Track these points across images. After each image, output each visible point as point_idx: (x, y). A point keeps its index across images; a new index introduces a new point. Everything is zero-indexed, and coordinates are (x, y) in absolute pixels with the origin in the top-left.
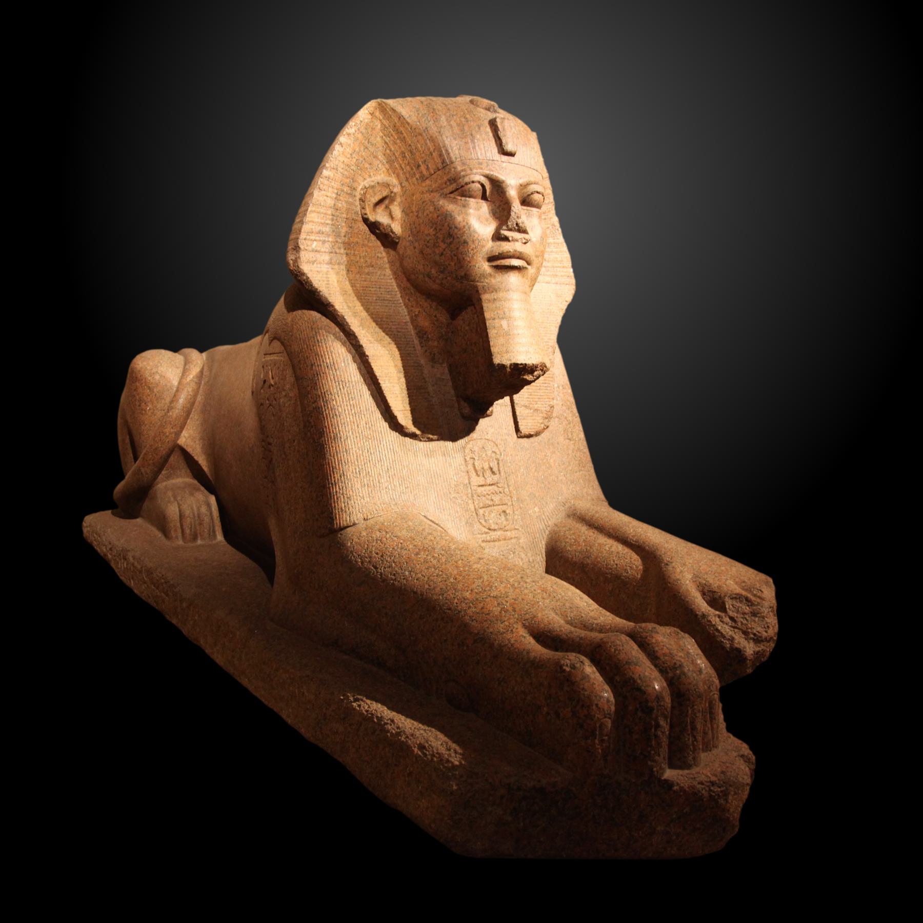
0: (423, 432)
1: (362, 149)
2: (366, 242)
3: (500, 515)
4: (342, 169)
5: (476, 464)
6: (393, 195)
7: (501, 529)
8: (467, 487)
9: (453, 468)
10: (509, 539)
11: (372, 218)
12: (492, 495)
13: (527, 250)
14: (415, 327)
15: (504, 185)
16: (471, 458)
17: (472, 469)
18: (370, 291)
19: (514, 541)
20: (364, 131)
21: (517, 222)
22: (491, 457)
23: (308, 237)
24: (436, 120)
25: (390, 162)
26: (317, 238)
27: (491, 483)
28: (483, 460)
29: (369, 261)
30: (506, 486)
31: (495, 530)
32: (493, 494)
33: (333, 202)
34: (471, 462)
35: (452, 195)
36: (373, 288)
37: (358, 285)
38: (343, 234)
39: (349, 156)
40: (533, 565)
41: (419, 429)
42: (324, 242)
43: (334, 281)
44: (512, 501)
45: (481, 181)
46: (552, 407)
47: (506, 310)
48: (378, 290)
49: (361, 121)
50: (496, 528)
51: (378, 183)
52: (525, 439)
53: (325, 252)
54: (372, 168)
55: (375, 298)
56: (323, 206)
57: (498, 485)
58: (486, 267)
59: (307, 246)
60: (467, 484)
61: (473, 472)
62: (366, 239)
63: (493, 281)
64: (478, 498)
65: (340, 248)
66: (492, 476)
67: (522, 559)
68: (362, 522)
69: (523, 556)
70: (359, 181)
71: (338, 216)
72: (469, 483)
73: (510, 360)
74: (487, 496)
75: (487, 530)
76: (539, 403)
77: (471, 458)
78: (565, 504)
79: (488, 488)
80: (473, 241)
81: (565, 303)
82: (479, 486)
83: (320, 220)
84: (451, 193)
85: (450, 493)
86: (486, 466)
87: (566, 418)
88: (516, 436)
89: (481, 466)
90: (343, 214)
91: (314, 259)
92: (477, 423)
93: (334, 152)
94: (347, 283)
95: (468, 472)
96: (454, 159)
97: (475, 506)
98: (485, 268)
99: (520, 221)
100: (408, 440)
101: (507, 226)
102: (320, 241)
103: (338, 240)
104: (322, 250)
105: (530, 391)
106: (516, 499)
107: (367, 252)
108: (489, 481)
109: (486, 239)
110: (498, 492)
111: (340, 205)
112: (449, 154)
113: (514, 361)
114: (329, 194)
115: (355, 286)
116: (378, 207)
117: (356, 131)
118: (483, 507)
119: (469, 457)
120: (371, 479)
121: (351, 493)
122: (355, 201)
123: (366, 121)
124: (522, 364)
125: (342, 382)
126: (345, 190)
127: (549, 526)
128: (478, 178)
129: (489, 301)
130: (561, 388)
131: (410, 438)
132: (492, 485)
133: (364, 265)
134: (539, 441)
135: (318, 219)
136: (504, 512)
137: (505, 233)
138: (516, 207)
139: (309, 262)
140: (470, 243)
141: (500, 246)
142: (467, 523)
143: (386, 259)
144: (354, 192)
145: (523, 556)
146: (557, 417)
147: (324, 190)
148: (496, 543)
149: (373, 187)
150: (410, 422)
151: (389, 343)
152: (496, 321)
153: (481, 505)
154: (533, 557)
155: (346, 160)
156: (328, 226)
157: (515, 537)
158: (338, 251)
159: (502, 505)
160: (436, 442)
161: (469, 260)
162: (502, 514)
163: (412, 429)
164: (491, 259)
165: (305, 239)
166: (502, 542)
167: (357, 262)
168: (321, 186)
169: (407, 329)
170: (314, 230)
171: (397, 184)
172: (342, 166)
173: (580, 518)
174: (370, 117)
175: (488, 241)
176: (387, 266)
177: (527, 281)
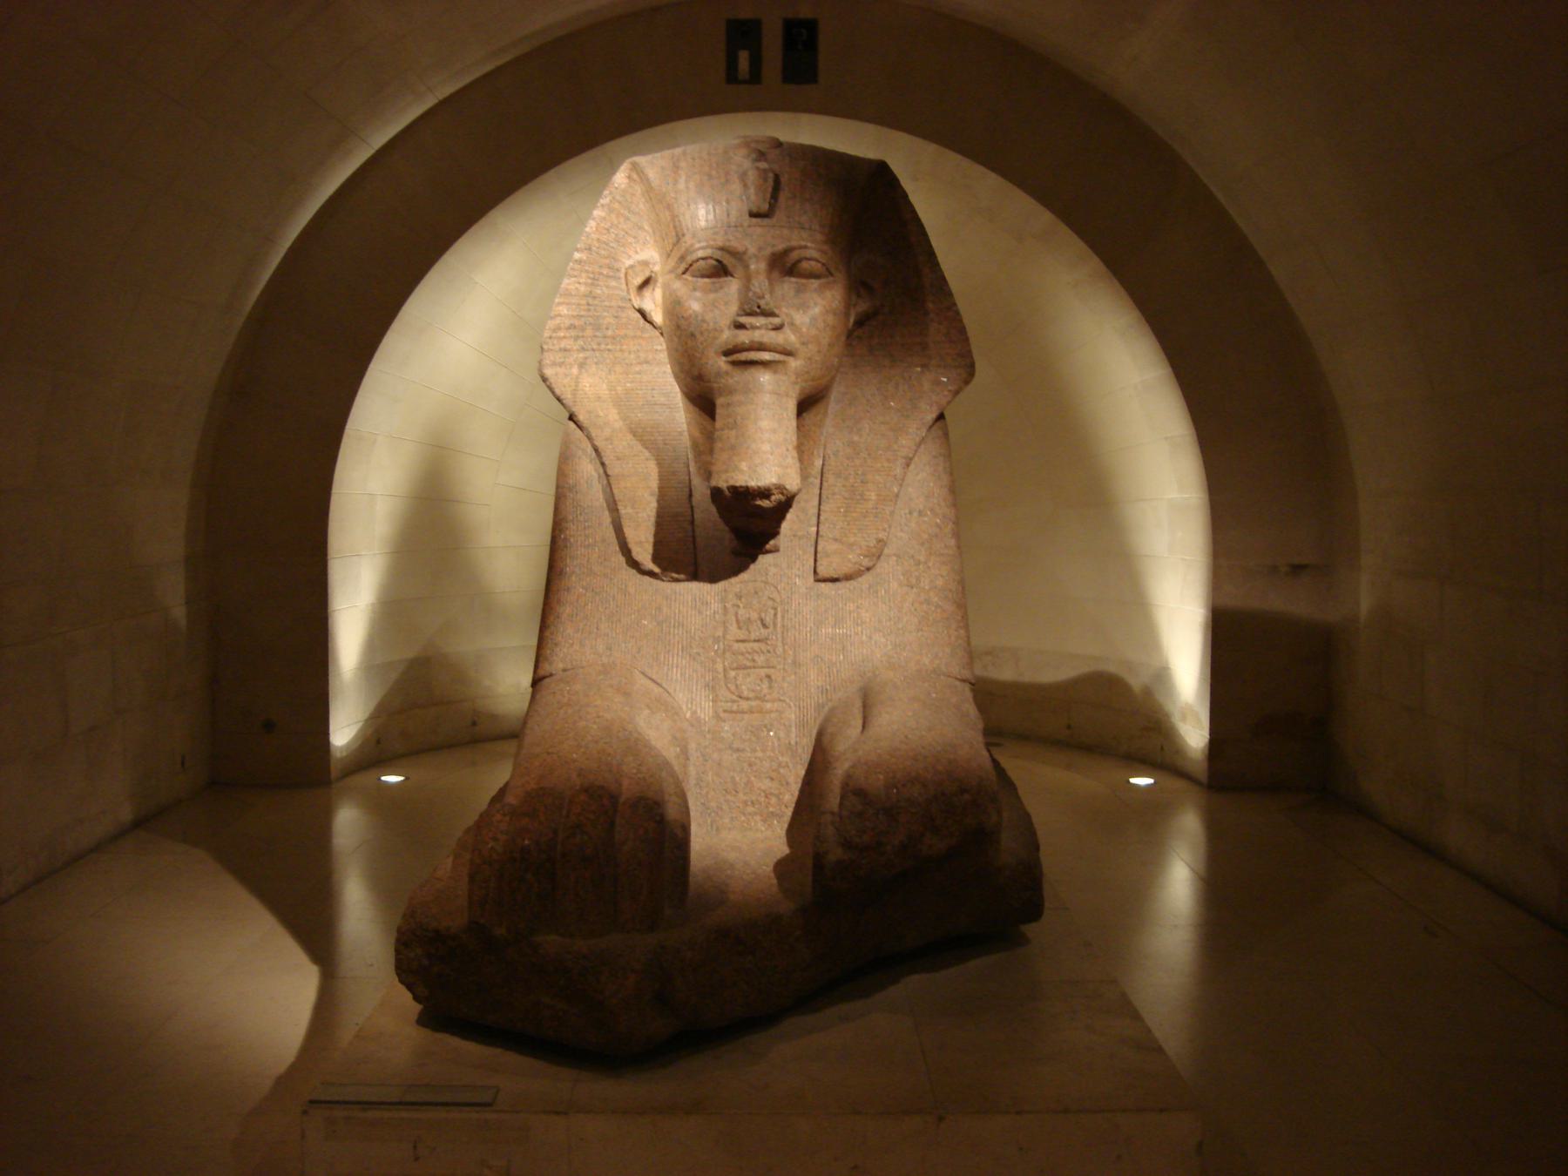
0: (664, 569)
1: (622, 220)
2: (639, 333)
3: (761, 680)
4: (598, 248)
5: (740, 613)
6: (653, 275)
7: (757, 698)
8: (719, 642)
9: (704, 616)
10: (767, 712)
11: (637, 307)
12: (755, 654)
13: (788, 337)
14: (690, 435)
15: (746, 257)
16: (734, 605)
17: (734, 618)
18: (637, 394)
19: (773, 715)
20: (621, 199)
21: (757, 303)
22: (764, 605)
23: (554, 335)
24: (676, 182)
25: (654, 232)
26: (568, 335)
27: (757, 638)
28: (751, 608)
29: (642, 355)
30: (780, 644)
31: (748, 699)
32: (757, 652)
33: (589, 289)
34: (732, 611)
35: (684, 276)
36: (641, 390)
37: (619, 388)
38: (604, 326)
39: (605, 232)
40: (794, 748)
41: (659, 566)
42: (576, 338)
43: (585, 386)
44: (784, 664)
45: (715, 257)
46: (880, 541)
47: (739, 418)
48: (650, 391)
49: (616, 188)
50: (751, 695)
51: (639, 262)
52: (830, 584)
53: (578, 350)
54: (638, 241)
55: (641, 403)
56: (575, 296)
57: (769, 642)
58: (722, 363)
59: (553, 345)
60: (719, 637)
61: (735, 625)
62: (639, 329)
63: (731, 381)
64: (734, 657)
65: (599, 344)
66: (762, 630)
67: (779, 739)
68: (561, 673)
69: (782, 735)
70: (624, 260)
71: (596, 305)
72: (724, 637)
73: (727, 482)
74: (747, 655)
75: (735, 698)
76: (860, 535)
77: (734, 605)
78: (864, 673)
79: (752, 644)
80: (702, 333)
81: (946, 393)
82: (738, 641)
83: (570, 313)
84: (684, 273)
85: (691, 647)
86: (754, 616)
87: (913, 556)
88: (812, 579)
89: (747, 616)
90: (604, 301)
91: (562, 360)
92: (754, 559)
93: (587, 229)
94: (605, 386)
95: (724, 623)
96: (685, 231)
97: (724, 666)
98: (720, 367)
99: (762, 303)
100: (647, 579)
101: (744, 311)
102: (571, 337)
103: (597, 334)
104: (575, 348)
105: (848, 519)
106: (790, 661)
107: (639, 345)
108: (753, 637)
109: (718, 328)
110: (765, 651)
111: (599, 292)
112: (681, 225)
113: (732, 483)
114: (581, 281)
115: (615, 390)
116: (645, 289)
117: (611, 201)
118: (737, 669)
119: (731, 603)
120: (589, 624)
121: (560, 638)
122: (621, 284)
123: (623, 186)
124: (741, 487)
125: (580, 506)
126: (605, 272)
127: (831, 700)
128: (708, 252)
129: (722, 406)
130: (915, 514)
131: (651, 577)
132: (758, 641)
133: (634, 362)
134: (852, 588)
135: (568, 311)
136: (768, 677)
137: (743, 320)
138: (756, 284)
139: (554, 364)
140: (698, 336)
141: (736, 336)
142: (707, 685)
143: (666, 353)
144: (618, 274)
145: (782, 735)
146: (898, 556)
147: (575, 276)
148: (746, 716)
149: (632, 267)
150: (650, 557)
151: (647, 459)
152: (726, 431)
153: (735, 665)
154: (798, 739)
155: (604, 238)
156: (583, 319)
157: (777, 711)
158: (595, 347)
159: (769, 667)
160: (686, 583)
161: (698, 355)
162: (766, 682)
163: (649, 565)
164: (727, 353)
165: (550, 338)
166: (756, 715)
167: (624, 359)
168: (572, 272)
169: (680, 440)
170: (562, 325)
171: (658, 260)
172: (597, 245)
173: (865, 696)
174: (627, 181)
175: (722, 331)
176: (667, 360)
177: (784, 378)
